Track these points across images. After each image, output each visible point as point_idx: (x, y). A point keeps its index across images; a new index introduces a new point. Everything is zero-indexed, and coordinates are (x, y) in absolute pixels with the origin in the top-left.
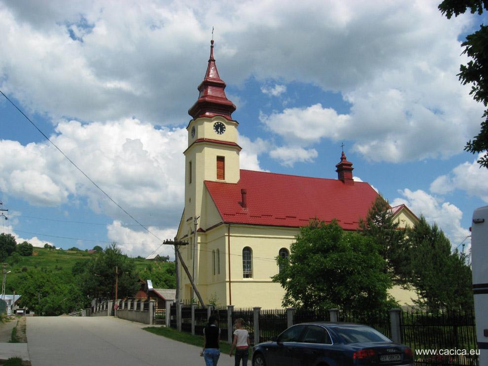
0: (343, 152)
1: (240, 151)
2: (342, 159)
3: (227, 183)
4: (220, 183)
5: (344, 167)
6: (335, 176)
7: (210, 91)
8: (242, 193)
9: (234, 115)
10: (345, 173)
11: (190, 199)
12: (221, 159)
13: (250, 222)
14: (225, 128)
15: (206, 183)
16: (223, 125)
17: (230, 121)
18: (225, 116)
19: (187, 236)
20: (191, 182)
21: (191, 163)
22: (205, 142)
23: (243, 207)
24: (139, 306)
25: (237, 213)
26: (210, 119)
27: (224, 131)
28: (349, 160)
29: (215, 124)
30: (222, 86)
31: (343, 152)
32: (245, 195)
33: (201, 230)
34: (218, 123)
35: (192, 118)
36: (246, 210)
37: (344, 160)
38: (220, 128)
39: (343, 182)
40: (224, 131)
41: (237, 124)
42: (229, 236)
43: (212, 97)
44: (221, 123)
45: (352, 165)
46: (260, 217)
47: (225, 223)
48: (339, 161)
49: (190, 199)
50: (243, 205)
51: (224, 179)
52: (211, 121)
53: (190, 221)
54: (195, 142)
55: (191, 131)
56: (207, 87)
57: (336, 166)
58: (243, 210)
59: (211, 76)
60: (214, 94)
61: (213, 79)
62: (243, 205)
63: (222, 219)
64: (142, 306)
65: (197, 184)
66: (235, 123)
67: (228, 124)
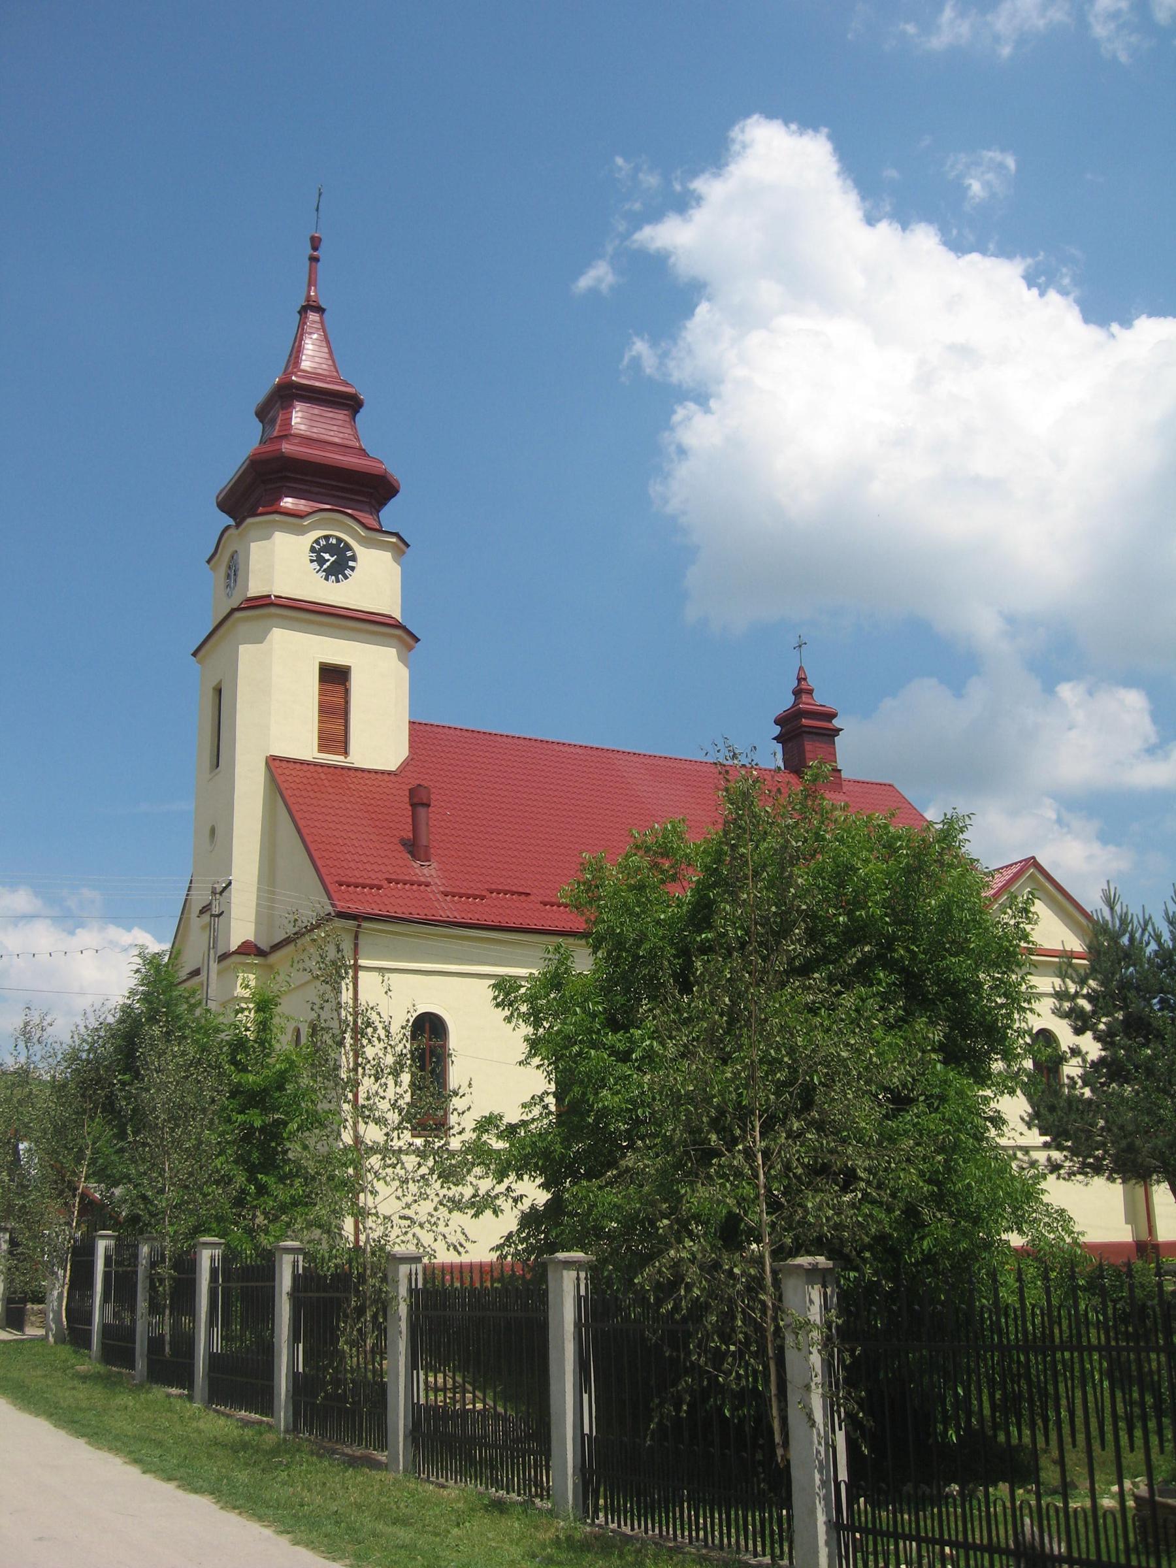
0: (801, 668)
2: (798, 693)
3: (357, 769)
4: (322, 765)
6: (772, 756)
8: (414, 805)
9: (390, 514)
10: (808, 746)
11: (213, 831)
13: (443, 915)
14: (354, 558)
15: (275, 764)
16: (348, 547)
17: (375, 533)
18: (349, 511)
20: (218, 766)
21: (219, 691)
22: (273, 610)
23: (415, 857)
25: (390, 881)
28: (822, 698)
29: (317, 541)
30: (350, 403)
31: (801, 668)
32: (422, 811)
33: (247, 949)
34: (327, 537)
35: (231, 522)
36: (428, 871)
37: (804, 698)
40: (353, 569)
41: (401, 546)
42: (357, 968)
43: (307, 440)
44: (339, 540)
45: (833, 715)
46: (483, 898)
47: (341, 915)
48: (786, 702)
49: (213, 831)
51: (346, 753)
52: (302, 531)
55: (222, 570)
56: (291, 406)
57: (778, 722)
59: (306, 364)
60: (318, 432)
61: (307, 374)
62: (414, 848)
63: (330, 898)
66: (394, 540)
67: (367, 543)
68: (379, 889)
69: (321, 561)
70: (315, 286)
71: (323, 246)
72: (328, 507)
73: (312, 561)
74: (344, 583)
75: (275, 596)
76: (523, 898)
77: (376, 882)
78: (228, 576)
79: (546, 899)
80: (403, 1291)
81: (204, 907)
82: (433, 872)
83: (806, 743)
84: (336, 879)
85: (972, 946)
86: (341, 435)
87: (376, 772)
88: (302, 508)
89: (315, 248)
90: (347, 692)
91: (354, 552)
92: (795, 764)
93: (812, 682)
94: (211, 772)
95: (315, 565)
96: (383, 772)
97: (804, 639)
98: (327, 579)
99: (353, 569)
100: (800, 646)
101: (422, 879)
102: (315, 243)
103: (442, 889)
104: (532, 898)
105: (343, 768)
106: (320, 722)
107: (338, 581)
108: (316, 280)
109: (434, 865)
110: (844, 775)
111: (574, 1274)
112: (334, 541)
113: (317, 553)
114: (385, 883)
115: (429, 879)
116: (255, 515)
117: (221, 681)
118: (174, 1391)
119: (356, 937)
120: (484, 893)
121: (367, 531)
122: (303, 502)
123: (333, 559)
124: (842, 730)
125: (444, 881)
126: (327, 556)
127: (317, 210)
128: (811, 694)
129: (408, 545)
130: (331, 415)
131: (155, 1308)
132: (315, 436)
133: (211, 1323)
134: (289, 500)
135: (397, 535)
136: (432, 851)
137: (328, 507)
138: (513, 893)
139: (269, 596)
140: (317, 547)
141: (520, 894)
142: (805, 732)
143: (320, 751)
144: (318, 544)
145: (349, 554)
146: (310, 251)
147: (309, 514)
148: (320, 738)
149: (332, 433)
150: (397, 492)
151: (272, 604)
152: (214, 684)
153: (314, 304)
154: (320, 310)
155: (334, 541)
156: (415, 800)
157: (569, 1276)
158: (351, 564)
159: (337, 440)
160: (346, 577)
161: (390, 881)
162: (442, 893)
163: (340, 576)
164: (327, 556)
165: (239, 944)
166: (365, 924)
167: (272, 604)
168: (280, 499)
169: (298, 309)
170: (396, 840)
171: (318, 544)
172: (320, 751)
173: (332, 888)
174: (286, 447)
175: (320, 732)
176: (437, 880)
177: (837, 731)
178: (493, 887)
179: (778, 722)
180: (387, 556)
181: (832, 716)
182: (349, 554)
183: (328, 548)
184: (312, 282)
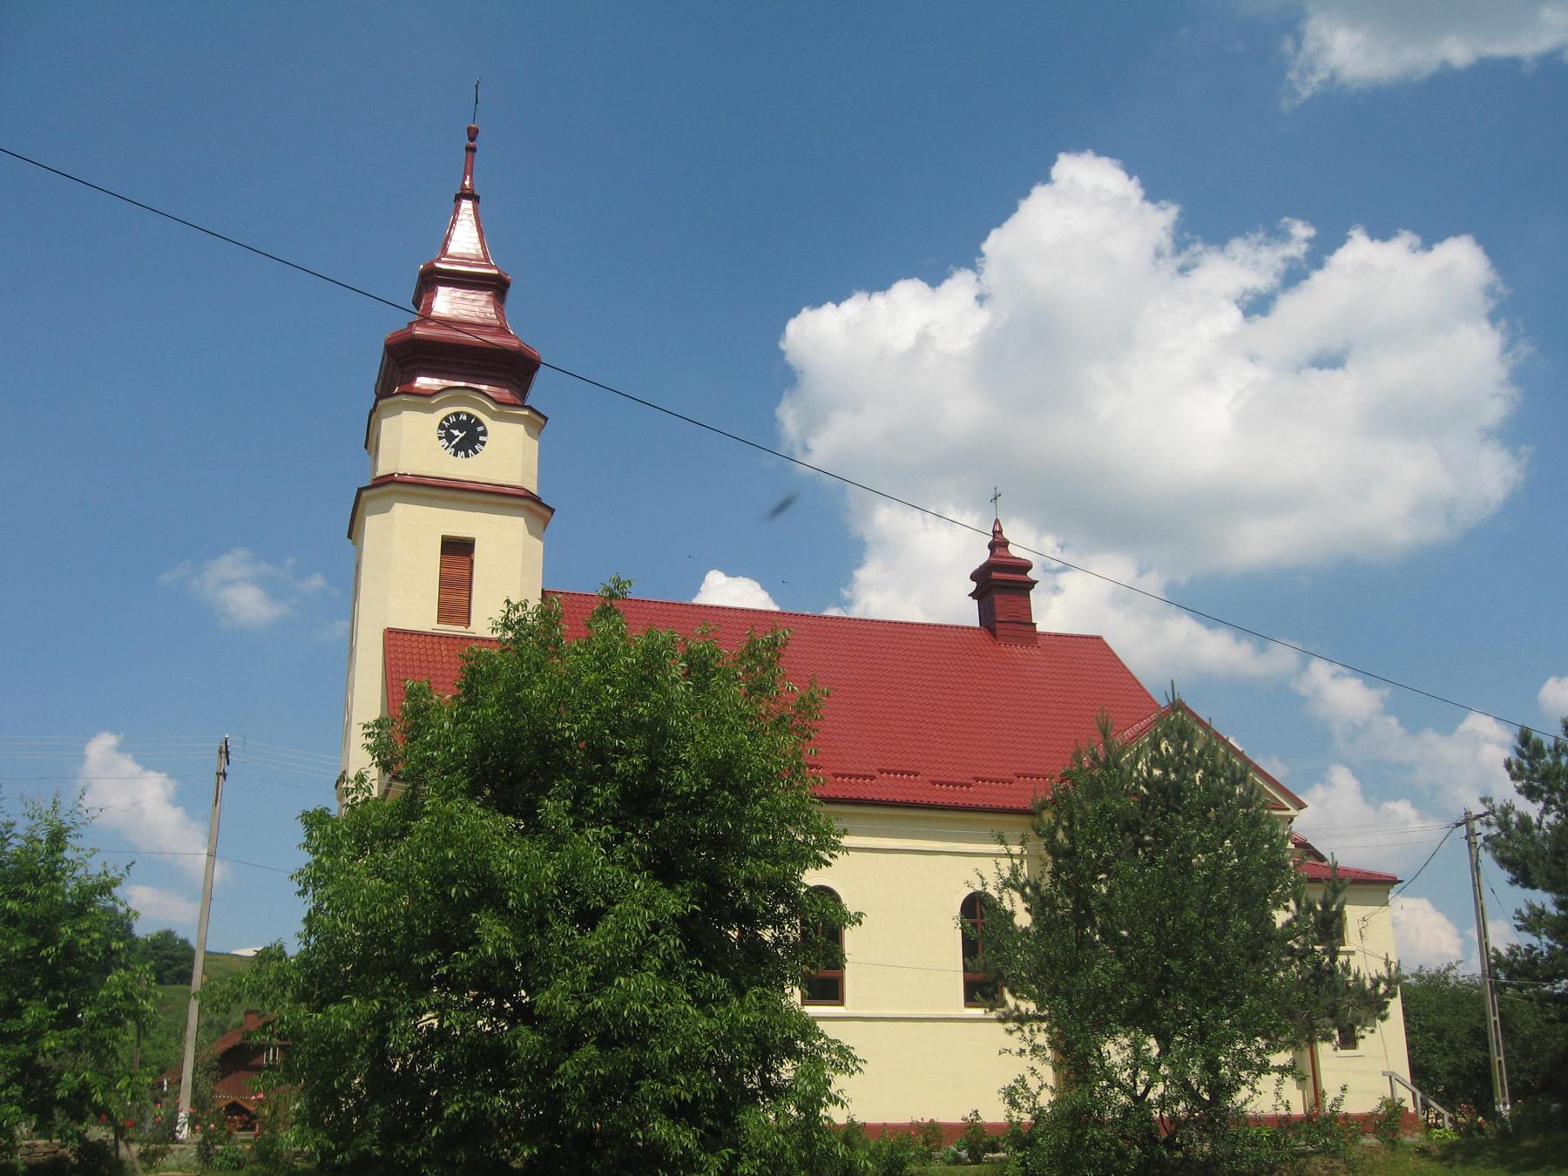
2: (992, 546)
4: (441, 636)
5: (995, 575)
6: (968, 613)
12: (457, 550)
14: (484, 433)
16: (479, 423)
18: (484, 388)
22: (393, 487)
27: (483, 443)
29: (446, 419)
34: (457, 415)
38: (466, 437)
40: (483, 443)
43: (445, 323)
44: (470, 416)
48: (983, 556)
52: (431, 409)
57: (973, 577)
61: (463, 260)
66: (526, 412)
67: (494, 416)
69: (450, 437)
73: (440, 438)
74: (474, 459)
89: (472, 139)
91: (485, 427)
93: (1007, 534)
95: (444, 442)
98: (456, 455)
100: (996, 498)
102: (473, 134)
105: (462, 638)
112: (465, 418)
113: (446, 430)
121: (499, 406)
123: (462, 435)
124: (1037, 582)
126: (456, 432)
128: (1007, 547)
130: (473, 297)
137: (462, 384)
140: (446, 424)
144: (448, 421)
145: (480, 429)
146: (467, 142)
147: (437, 393)
154: (474, 198)
155: (465, 418)
158: (481, 438)
163: (470, 451)
164: (456, 432)
168: (414, 380)
171: (448, 421)
177: (1032, 583)
179: (973, 577)
180: (519, 429)
182: (480, 429)
183: (459, 425)
184: (469, 170)
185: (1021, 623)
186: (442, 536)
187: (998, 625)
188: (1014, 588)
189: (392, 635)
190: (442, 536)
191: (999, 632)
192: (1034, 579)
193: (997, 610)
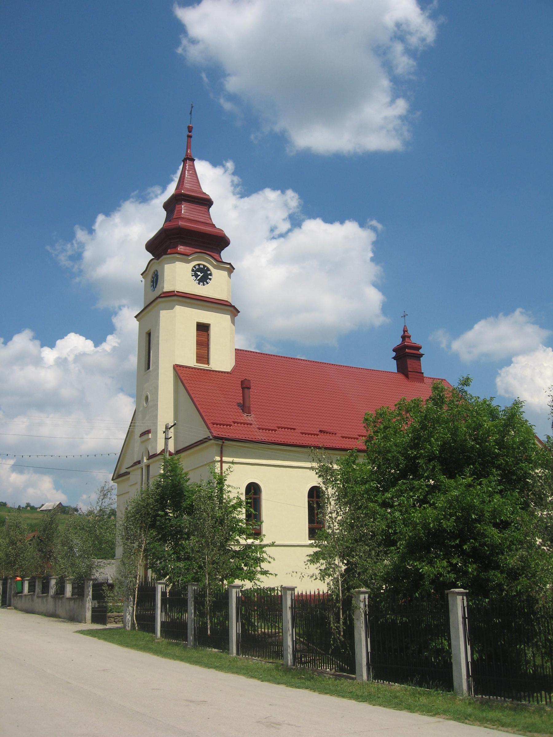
1: (236, 315)
2: (404, 337)
3: (213, 371)
4: (198, 369)
6: (392, 366)
7: (184, 209)
8: (243, 388)
9: (226, 255)
14: (211, 275)
15: (177, 368)
16: (208, 269)
19: (139, 462)
20: (149, 368)
21: (149, 334)
24: (61, 590)
25: (234, 423)
26: (185, 257)
28: (415, 340)
29: (195, 267)
32: (246, 390)
34: (199, 265)
36: (250, 419)
39: (407, 376)
40: (210, 279)
42: (222, 462)
44: (204, 266)
46: (275, 431)
47: (216, 438)
48: (398, 341)
50: (244, 408)
51: (208, 363)
52: (188, 262)
53: (145, 437)
54: (159, 297)
55: (150, 278)
56: (181, 204)
57: (394, 350)
58: (245, 418)
59: (187, 185)
62: (244, 408)
64: (69, 589)
65: (161, 371)
66: (229, 266)
67: (216, 267)
68: (230, 426)
69: (196, 276)
70: (190, 149)
71: (193, 130)
72: (198, 250)
73: (192, 276)
75: (177, 291)
76: (292, 430)
77: (228, 423)
78: (153, 281)
79: (303, 431)
80: (362, 605)
81: (142, 433)
82: (252, 419)
83: (408, 360)
84: (212, 421)
85: (533, 458)
86: (204, 218)
87: (222, 372)
88: (187, 251)
89: (190, 132)
90: (208, 335)
91: (211, 271)
92: (402, 369)
93: (410, 332)
94: (145, 371)
95: (194, 277)
96: (225, 372)
97: (406, 313)
99: (210, 279)
100: (404, 316)
101: (248, 422)
102: (190, 129)
103: (257, 426)
104: (296, 431)
105: (207, 370)
106: (197, 349)
107: (204, 285)
108: (190, 146)
109: (253, 415)
110: (425, 375)
111: (461, 597)
112: (202, 267)
113: (194, 272)
114: (232, 424)
115: (251, 422)
116: (166, 254)
117: (150, 330)
118: (216, 650)
119: (222, 448)
120: (276, 428)
122: (188, 248)
123: (202, 275)
124: (424, 354)
125: (258, 423)
126: (199, 273)
127: (191, 113)
129: (234, 269)
130: (199, 208)
131: (200, 613)
132: (192, 218)
133: (237, 621)
134: (182, 247)
135: (230, 264)
136: (251, 409)
137: (198, 250)
138: (288, 428)
139: (174, 291)
140: (195, 269)
141: (291, 429)
142: (407, 355)
143: (197, 362)
144: (195, 268)
145: (209, 272)
146: (188, 133)
148: (197, 357)
149: (200, 217)
150: (229, 244)
151: (175, 295)
152: (147, 330)
153: (190, 157)
155: (202, 267)
156: (244, 386)
157: (459, 598)
158: (210, 277)
159: (202, 220)
160: (207, 283)
161: (234, 423)
162: (258, 428)
164: (199, 273)
165: (161, 450)
166: (227, 443)
167: (175, 295)
168: (177, 247)
169: (183, 159)
170: (236, 404)
171: (195, 268)
172: (197, 362)
173: (210, 425)
174: (181, 223)
175: (197, 353)
176: (255, 422)
177: (422, 355)
178: (279, 425)
179: (394, 350)
180: (226, 273)
181: (419, 348)
182: (209, 272)
183: (200, 270)
184: (188, 146)
185: (416, 372)
186: (197, 322)
187: (409, 373)
188: (415, 357)
189: (177, 368)
190: (197, 322)
191: (410, 376)
192: (423, 353)
193: (409, 366)
